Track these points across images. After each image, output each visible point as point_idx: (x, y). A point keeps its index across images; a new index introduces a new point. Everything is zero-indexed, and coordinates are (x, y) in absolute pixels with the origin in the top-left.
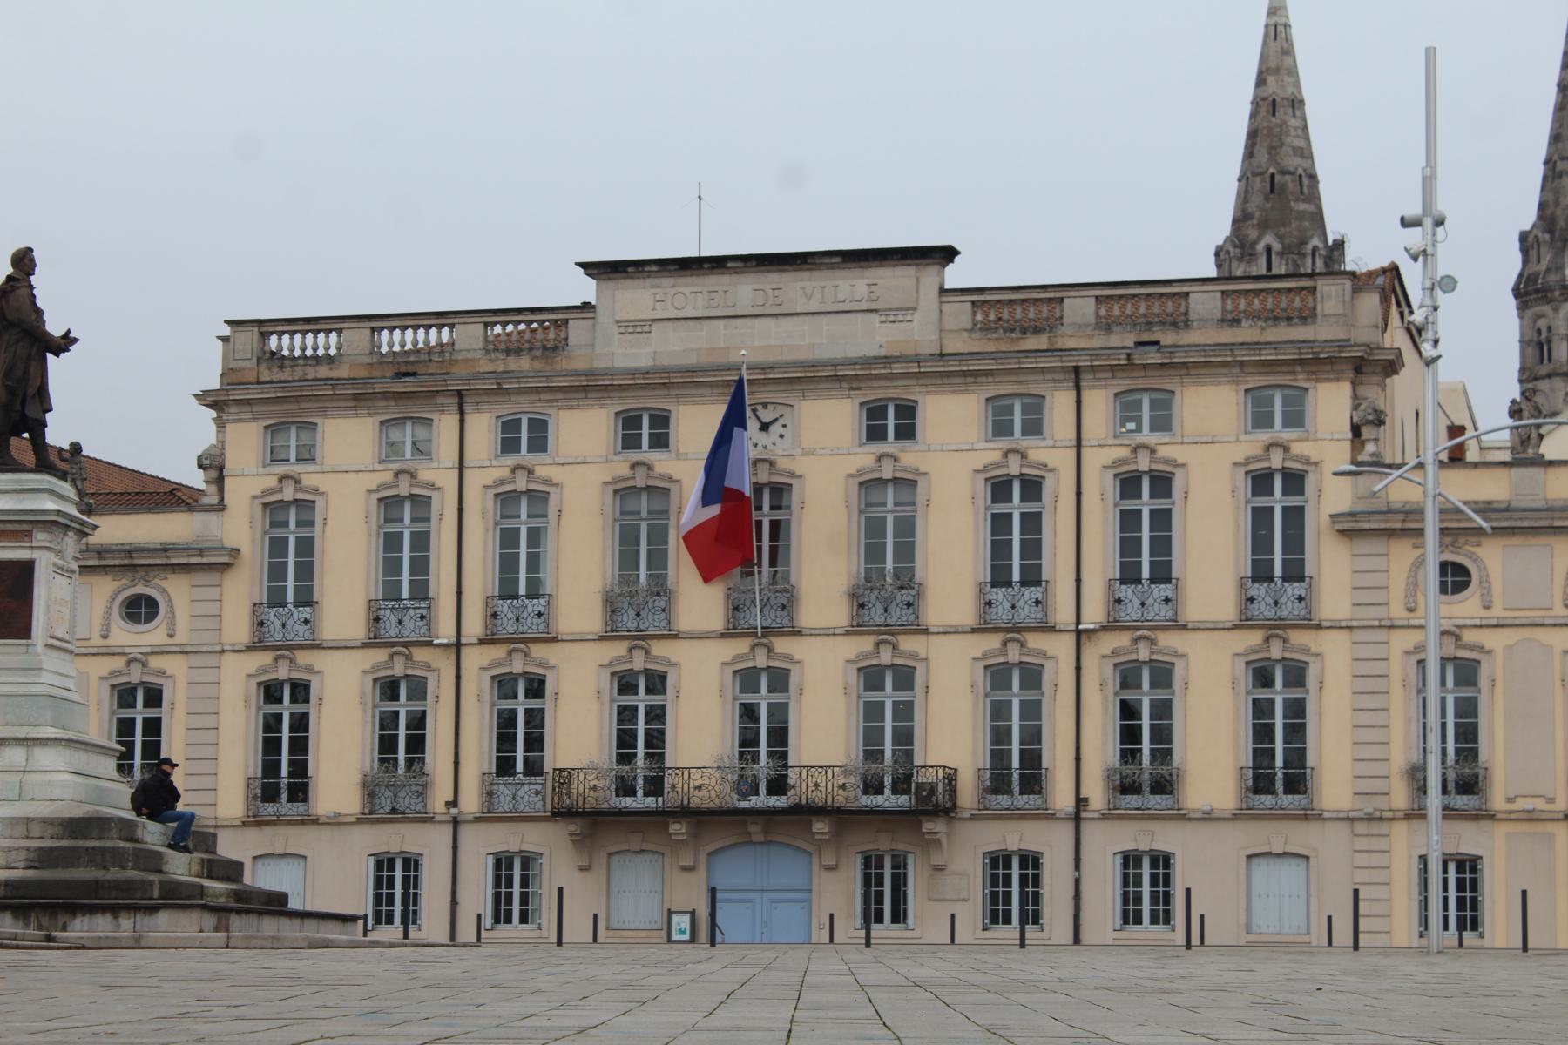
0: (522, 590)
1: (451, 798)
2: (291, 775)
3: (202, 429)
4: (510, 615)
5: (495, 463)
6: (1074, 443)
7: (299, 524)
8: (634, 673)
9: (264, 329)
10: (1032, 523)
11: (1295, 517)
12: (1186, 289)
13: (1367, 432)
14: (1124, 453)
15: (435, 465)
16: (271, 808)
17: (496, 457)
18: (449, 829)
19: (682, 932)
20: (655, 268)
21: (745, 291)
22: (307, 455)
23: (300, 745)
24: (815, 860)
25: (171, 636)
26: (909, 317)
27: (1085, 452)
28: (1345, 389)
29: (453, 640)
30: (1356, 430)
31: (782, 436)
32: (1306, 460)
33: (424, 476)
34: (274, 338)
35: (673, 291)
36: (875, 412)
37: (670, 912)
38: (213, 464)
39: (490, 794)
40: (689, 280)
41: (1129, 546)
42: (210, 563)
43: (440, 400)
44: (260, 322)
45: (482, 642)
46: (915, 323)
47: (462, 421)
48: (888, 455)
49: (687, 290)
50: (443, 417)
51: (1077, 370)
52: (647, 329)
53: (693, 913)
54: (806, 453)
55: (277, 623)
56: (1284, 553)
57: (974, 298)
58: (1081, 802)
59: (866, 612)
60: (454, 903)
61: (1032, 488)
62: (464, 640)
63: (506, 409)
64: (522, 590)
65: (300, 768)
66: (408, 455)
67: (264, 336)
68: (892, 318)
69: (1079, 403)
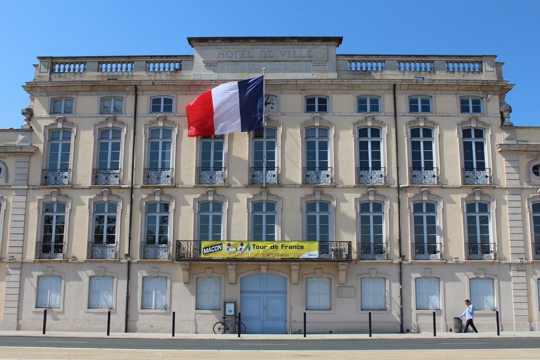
0: (160, 166)
1: (127, 252)
2: (56, 241)
3: (25, 100)
4: (155, 176)
5: (150, 115)
6: (393, 114)
7: (64, 138)
8: (208, 203)
9: (53, 61)
11: (480, 146)
12: (433, 59)
13: (505, 114)
15: (124, 115)
16: (47, 255)
17: (150, 113)
18: (126, 266)
19: (230, 311)
20: (220, 41)
21: (257, 51)
22: (69, 111)
23: (60, 229)
24: (288, 281)
25: (6, 182)
26: (324, 64)
27: (398, 118)
28: (497, 97)
29: (130, 186)
30: (501, 113)
31: (272, 108)
32: (485, 124)
33: (119, 119)
34: (57, 66)
35: (227, 50)
36: (310, 101)
37: (225, 303)
38: (29, 113)
39: (145, 252)
40: (233, 47)
41: (415, 155)
42: (26, 153)
43: (127, 89)
44: (52, 58)
45: (142, 187)
46: (327, 66)
47: (136, 98)
48: (317, 116)
49: (233, 51)
50: (128, 96)
53: (235, 303)
54: (282, 115)
55: (53, 178)
56: (477, 160)
57: (350, 59)
58: (402, 256)
59: (310, 178)
60: (128, 297)
62: (134, 187)
64: (160, 166)
65: (60, 239)
66: (112, 112)
67: (53, 64)
68: (317, 64)
69: (395, 99)
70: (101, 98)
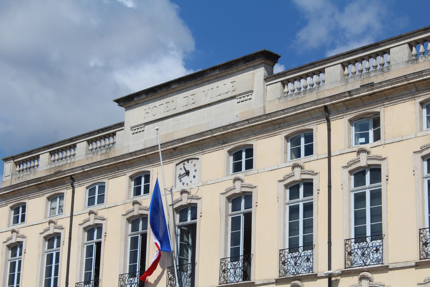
10: (309, 208)
14: (354, 156)
41: (359, 218)
51: (326, 107)
52: (142, 129)
61: (309, 186)
63: (89, 182)
69: (329, 130)
70: (49, 198)
